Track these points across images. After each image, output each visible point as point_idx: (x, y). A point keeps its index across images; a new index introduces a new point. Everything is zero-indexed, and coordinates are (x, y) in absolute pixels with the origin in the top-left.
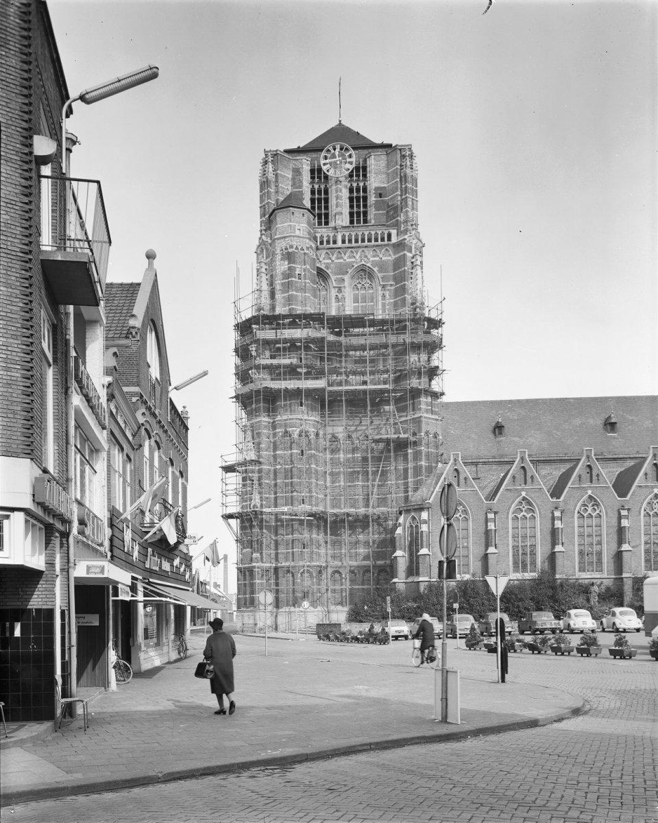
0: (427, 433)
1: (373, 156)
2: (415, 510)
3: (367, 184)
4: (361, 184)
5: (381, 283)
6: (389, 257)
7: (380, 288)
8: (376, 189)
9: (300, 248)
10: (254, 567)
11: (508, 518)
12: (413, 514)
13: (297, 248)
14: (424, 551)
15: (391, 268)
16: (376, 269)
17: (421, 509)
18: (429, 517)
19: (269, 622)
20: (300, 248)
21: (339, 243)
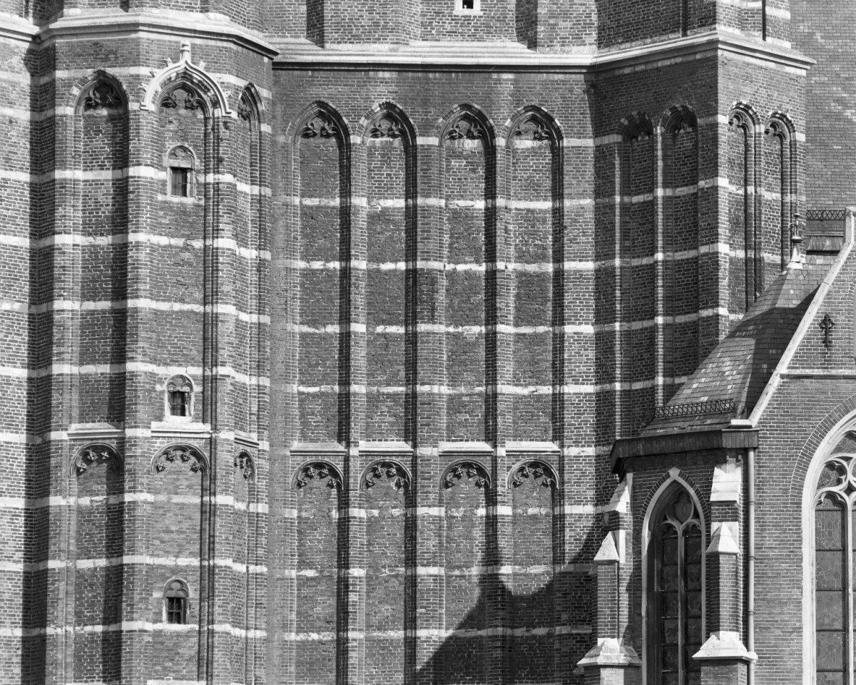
0: (743, 115)
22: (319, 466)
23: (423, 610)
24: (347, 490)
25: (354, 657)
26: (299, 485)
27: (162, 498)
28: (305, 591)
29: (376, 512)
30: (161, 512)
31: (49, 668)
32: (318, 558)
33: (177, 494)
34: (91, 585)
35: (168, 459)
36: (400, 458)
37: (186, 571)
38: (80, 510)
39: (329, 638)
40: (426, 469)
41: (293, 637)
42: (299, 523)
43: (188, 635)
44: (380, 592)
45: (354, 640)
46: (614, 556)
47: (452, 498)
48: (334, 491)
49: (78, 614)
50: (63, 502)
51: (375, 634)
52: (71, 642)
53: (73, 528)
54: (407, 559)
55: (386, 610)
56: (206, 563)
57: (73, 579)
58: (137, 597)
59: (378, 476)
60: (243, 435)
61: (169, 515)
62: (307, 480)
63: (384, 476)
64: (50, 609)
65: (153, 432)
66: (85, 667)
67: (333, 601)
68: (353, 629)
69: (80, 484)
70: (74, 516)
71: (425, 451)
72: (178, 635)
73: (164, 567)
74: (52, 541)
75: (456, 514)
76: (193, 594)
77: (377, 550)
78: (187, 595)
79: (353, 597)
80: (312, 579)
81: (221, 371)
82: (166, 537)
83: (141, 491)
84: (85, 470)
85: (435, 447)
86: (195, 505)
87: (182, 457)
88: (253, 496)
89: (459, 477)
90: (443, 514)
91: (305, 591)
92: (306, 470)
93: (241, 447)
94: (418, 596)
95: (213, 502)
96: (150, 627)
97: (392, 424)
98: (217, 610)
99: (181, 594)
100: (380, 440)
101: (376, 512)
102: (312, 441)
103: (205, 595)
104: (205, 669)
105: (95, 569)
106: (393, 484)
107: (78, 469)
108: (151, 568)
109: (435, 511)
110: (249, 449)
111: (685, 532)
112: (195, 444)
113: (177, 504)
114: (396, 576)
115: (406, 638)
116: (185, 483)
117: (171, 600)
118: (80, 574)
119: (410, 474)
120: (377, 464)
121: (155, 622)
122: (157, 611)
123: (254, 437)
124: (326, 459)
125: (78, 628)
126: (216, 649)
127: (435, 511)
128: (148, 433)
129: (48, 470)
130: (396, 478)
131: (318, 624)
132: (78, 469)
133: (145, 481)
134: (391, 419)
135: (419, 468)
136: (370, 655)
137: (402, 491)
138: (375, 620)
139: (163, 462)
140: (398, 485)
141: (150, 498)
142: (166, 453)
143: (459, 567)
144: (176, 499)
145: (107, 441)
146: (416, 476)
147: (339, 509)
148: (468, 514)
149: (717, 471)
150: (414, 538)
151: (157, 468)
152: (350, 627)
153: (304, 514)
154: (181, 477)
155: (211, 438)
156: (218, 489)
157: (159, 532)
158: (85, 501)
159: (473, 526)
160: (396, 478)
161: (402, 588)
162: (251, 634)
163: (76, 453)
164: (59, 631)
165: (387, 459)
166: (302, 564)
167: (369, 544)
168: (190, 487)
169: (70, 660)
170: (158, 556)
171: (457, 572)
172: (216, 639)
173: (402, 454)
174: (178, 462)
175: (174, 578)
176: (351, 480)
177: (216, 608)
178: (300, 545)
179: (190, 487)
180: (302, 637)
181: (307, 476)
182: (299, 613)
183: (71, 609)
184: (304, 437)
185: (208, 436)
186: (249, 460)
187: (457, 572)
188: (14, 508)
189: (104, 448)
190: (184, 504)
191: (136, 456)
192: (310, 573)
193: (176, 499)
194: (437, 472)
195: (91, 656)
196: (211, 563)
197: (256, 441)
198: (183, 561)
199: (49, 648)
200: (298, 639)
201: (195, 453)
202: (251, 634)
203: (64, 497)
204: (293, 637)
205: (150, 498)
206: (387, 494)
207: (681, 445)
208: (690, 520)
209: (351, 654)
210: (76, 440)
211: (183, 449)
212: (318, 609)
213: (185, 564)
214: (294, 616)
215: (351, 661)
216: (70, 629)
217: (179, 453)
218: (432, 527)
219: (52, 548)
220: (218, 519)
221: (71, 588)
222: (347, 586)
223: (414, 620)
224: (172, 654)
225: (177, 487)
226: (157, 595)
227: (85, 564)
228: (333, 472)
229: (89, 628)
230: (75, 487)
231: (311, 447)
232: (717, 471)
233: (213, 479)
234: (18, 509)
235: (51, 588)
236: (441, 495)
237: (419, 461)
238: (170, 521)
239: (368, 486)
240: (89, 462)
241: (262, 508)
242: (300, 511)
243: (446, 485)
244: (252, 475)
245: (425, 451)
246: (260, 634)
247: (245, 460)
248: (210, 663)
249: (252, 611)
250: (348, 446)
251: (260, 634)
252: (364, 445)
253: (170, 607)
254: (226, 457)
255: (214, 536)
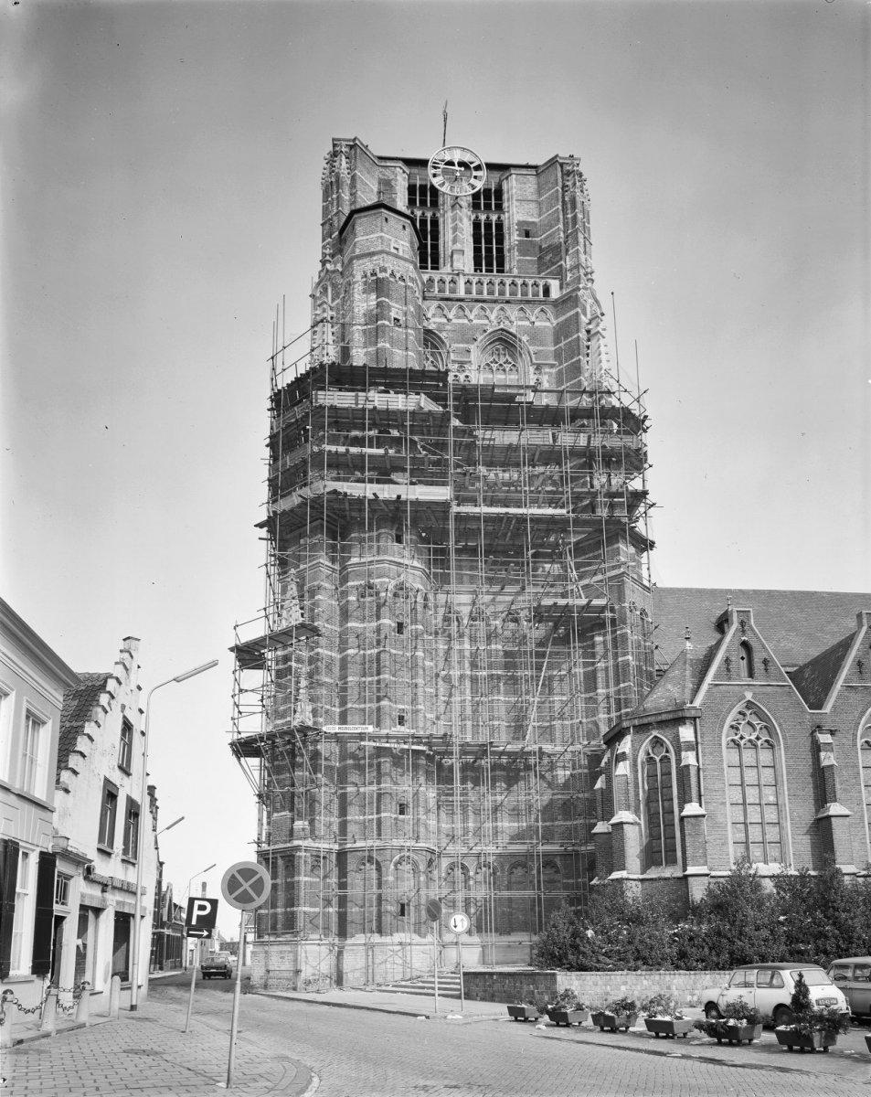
1: (514, 176)
2: (662, 724)
3: (502, 217)
4: (494, 218)
5: (534, 361)
6: (546, 322)
7: (532, 369)
8: (520, 223)
9: (398, 275)
10: (298, 848)
11: (855, 745)
12: (655, 733)
13: (392, 275)
14: (692, 809)
15: (550, 338)
16: (525, 338)
17: (680, 721)
18: (696, 737)
19: (326, 966)
20: (398, 275)
21: (461, 293)
46: (625, 773)
81: (420, 707)
111: (661, 760)
149: (680, 728)
207: (659, 718)
208: (664, 754)
232: (680, 728)
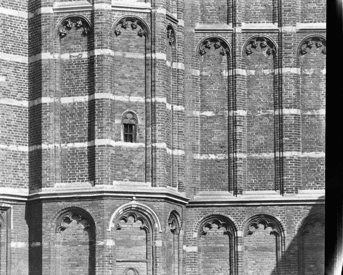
22: (214, 40)
23: (288, 139)
24: (234, 56)
25: (240, 171)
26: (201, 53)
27: (119, 54)
28: (206, 126)
29: (253, 72)
30: (119, 63)
31: (44, 172)
32: (214, 104)
33: (128, 51)
34: (72, 115)
35: (123, 27)
36: (270, 34)
37: (136, 106)
38: (62, 63)
39: (223, 158)
40: (288, 42)
41: (198, 157)
42: (201, 79)
43: (138, 150)
44: (256, 127)
45: (241, 159)
47: (305, 62)
48: (225, 58)
49: (63, 135)
50: (51, 57)
51: (254, 155)
52: (58, 154)
53: (58, 75)
54: (275, 103)
55: (261, 139)
56: (149, 100)
57: (59, 110)
58: (105, 122)
59: (254, 47)
60: (170, 14)
61: (124, 66)
62: (207, 50)
63: (259, 47)
64: (44, 131)
65: (112, 7)
66: (69, 172)
67: (225, 133)
68: (240, 152)
69: (62, 45)
70: (58, 67)
71: (288, 29)
72: (132, 150)
73: (121, 102)
74: (44, 84)
75: (308, 73)
76: (141, 122)
77: (253, 97)
78: (137, 122)
79: (239, 130)
80: (210, 118)
82: (122, 81)
83: (106, 48)
84: (65, 34)
85: (295, 26)
86: (141, 60)
87: (132, 25)
88: (175, 57)
89: (310, 47)
90: (299, 73)
91: (206, 126)
92: (205, 43)
93: (169, 22)
94: (284, 128)
95: (153, 58)
96: (113, 143)
97: (263, 11)
98: (158, 133)
99: (133, 122)
100: (255, 23)
101: (253, 72)
102: (209, 23)
103: (149, 122)
104: (150, 174)
105: (74, 103)
106: (264, 53)
107: (60, 34)
108: (113, 102)
109: (295, 71)
110: (173, 24)
112: (140, 16)
113: (129, 59)
114: (268, 116)
115: (275, 158)
116: (134, 44)
117: (126, 125)
118: (64, 108)
119: (277, 46)
120: (254, 39)
121: (116, 140)
122: (117, 133)
123: (175, 16)
124: (219, 35)
125: (63, 145)
126: (158, 160)
127: (295, 71)
128: (109, 7)
129: (40, 34)
130: (266, 49)
131: (215, 148)
132: (60, 34)
133: (109, 41)
134: (263, 8)
135: (283, 40)
136: (251, 170)
137: (271, 57)
138: (253, 146)
139: (119, 28)
140: (268, 53)
141: (112, 53)
142: (121, 22)
143: (310, 109)
144: (128, 55)
145: (81, 14)
146: (281, 46)
147: (229, 69)
148: (316, 73)
150: (280, 89)
151: (115, 32)
152: (238, 150)
153: (204, 73)
154: (131, 40)
155: (151, 13)
156: (157, 48)
157: (118, 78)
158: (66, 56)
159: (320, 81)
160: (266, 49)
161: (272, 124)
162: (176, 152)
163: (59, 23)
164: (51, 146)
165: (261, 35)
166: (204, 108)
167: (249, 94)
168: (137, 47)
169: (58, 167)
170: (117, 94)
171: (309, 113)
172: (157, 153)
173: (271, 31)
174: (129, 29)
175: (128, 110)
176: (237, 49)
177: (157, 131)
178: (202, 94)
179: (137, 47)
180: (204, 157)
181: (206, 47)
182: (202, 141)
183: (58, 131)
184: (203, 21)
185: (149, 11)
186: (173, 32)
187: (309, 113)
188: (16, 62)
189: (77, 19)
190: (134, 59)
191: (102, 23)
192: (209, 114)
193: (128, 55)
194: (296, 42)
195: (73, 164)
196: (153, 100)
197: (176, 18)
198: (134, 99)
199: (44, 158)
200: (202, 158)
201: (141, 23)
202: (176, 152)
203: (52, 53)
204: (198, 157)
205: (112, 53)
206: (260, 59)
209: (239, 168)
210: (57, 13)
211: (132, 19)
212: (215, 138)
213: (135, 101)
214: (199, 143)
215: (239, 173)
216: (57, 145)
217: (130, 23)
218: (293, 81)
219: (44, 89)
220: (157, 70)
221: (57, 117)
222: (235, 122)
223: (281, 145)
224: (128, 163)
225: (129, 47)
226: (118, 121)
227: (66, 100)
228: (224, 44)
229: (70, 145)
230: (59, 47)
231: (209, 27)
233: (153, 41)
234: (19, 63)
235: (44, 116)
236: (298, 60)
237: (283, 36)
238: (124, 70)
239: (248, 54)
240: (69, 28)
241: (180, 66)
242: (201, 71)
243: (302, 53)
244: (174, 42)
245: (288, 29)
246: (181, 152)
247: (170, 31)
248: (153, 170)
249: (176, 137)
250: (234, 25)
251: (181, 152)
252: (245, 26)
253: (126, 131)
254: (161, 26)
255: (154, 81)
